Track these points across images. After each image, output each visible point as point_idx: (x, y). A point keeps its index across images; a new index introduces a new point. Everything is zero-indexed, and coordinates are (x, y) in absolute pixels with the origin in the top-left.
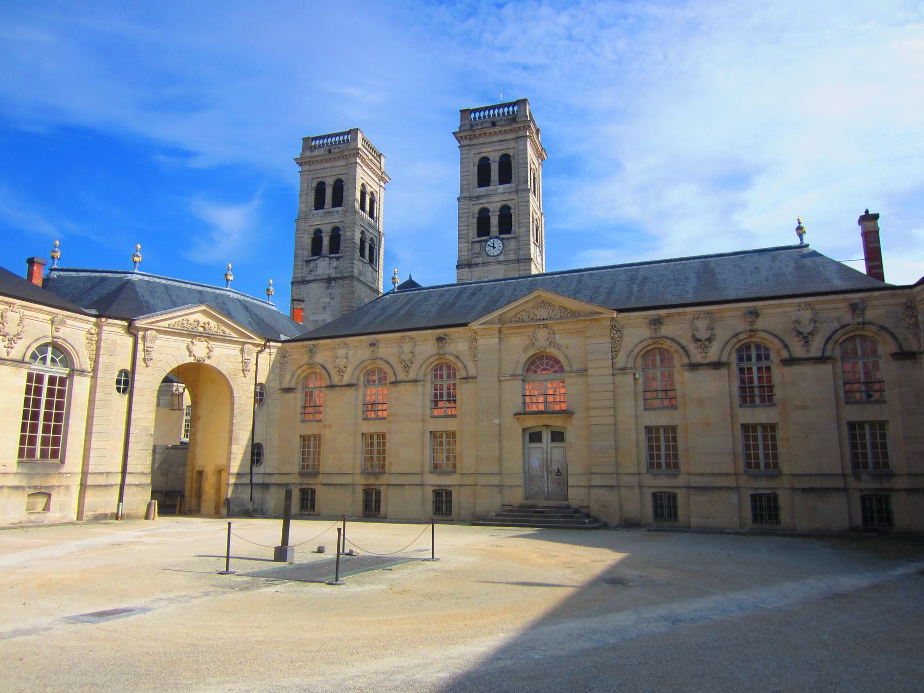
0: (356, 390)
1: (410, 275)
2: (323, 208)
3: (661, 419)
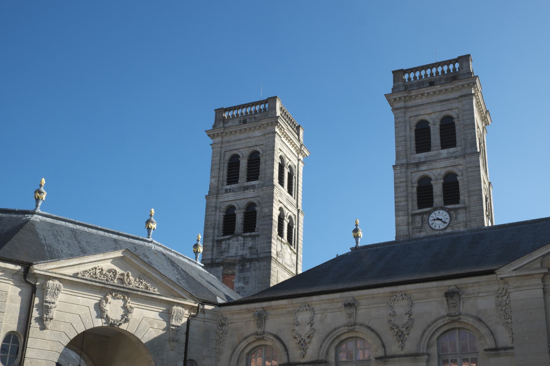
2: (236, 182)
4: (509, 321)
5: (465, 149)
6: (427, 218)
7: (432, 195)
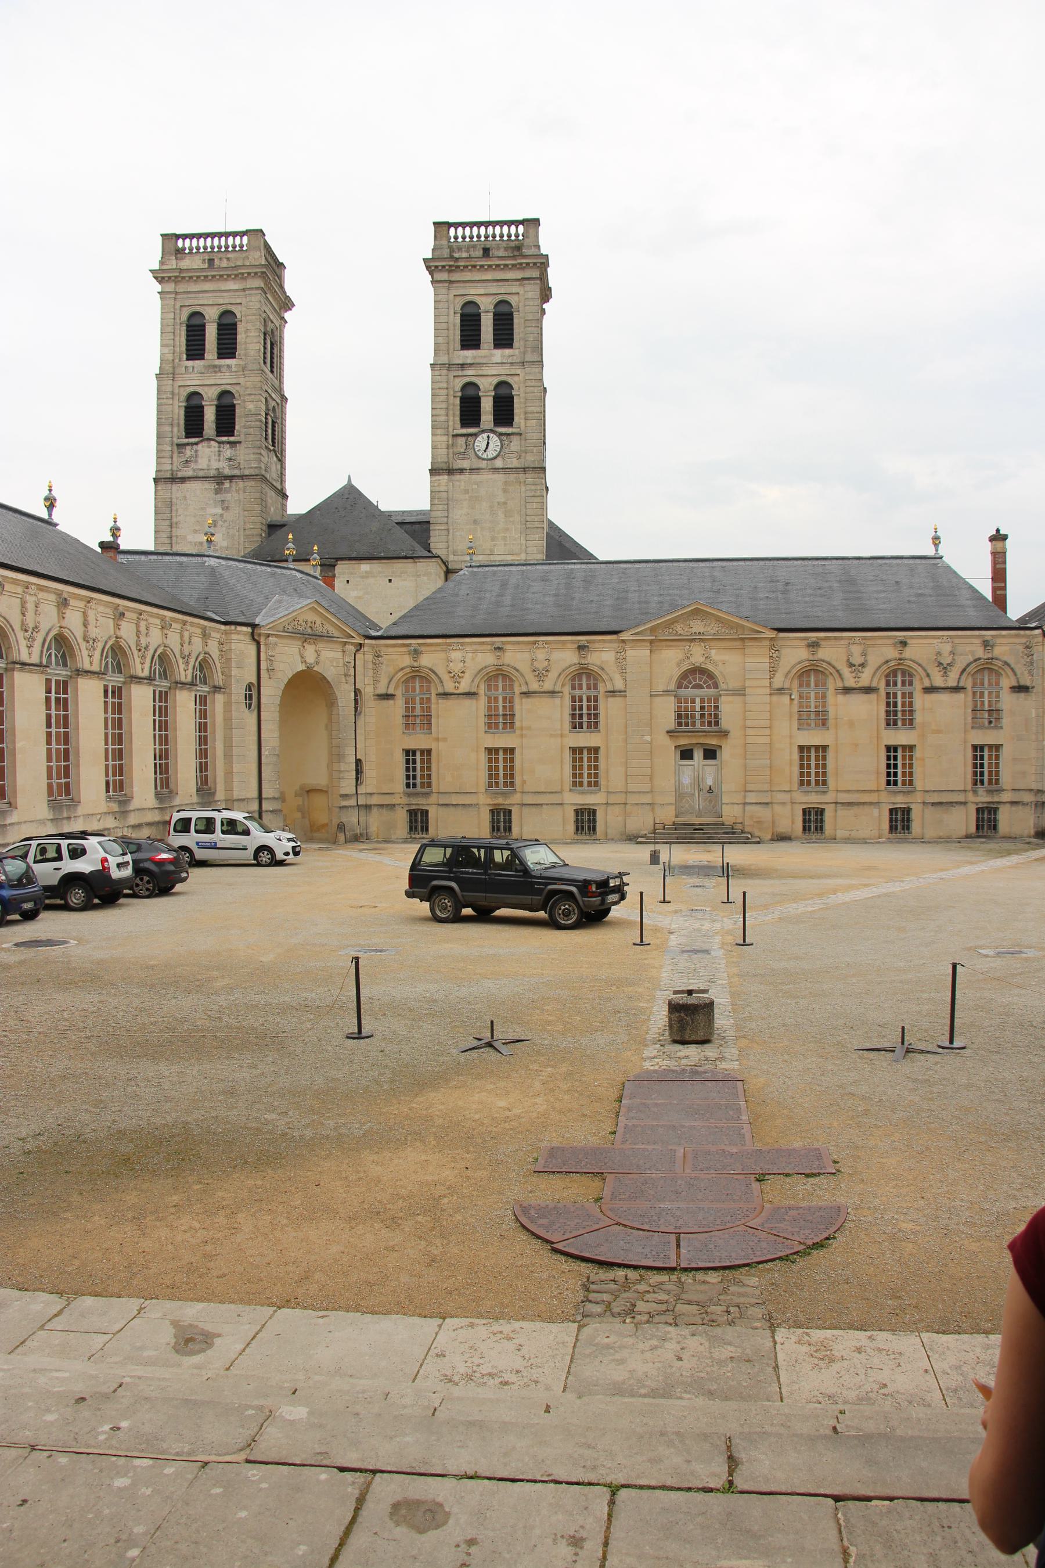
0: (477, 699)
3: (814, 738)
5: (524, 353)
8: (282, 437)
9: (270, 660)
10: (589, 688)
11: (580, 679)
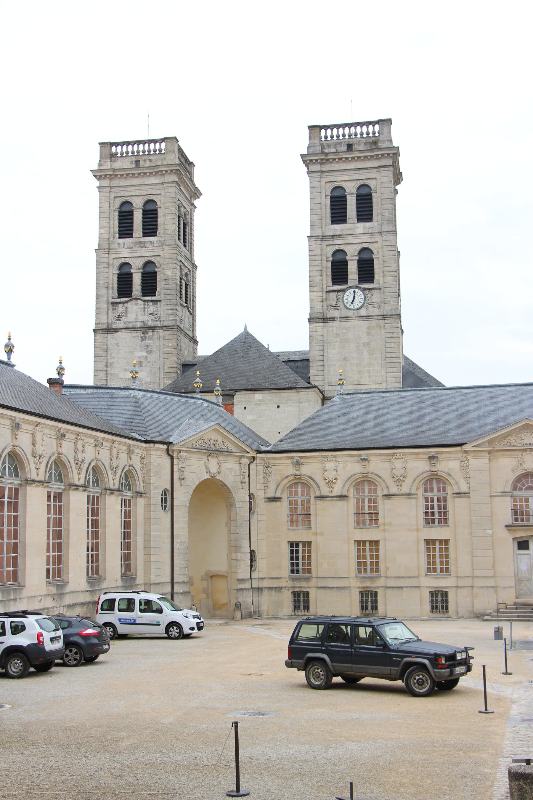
1: (246, 326)
4: (468, 476)
5: (382, 225)
6: (342, 296)
7: (347, 272)
8: (193, 296)
9: (181, 470)
10: (439, 491)
11: (431, 484)
